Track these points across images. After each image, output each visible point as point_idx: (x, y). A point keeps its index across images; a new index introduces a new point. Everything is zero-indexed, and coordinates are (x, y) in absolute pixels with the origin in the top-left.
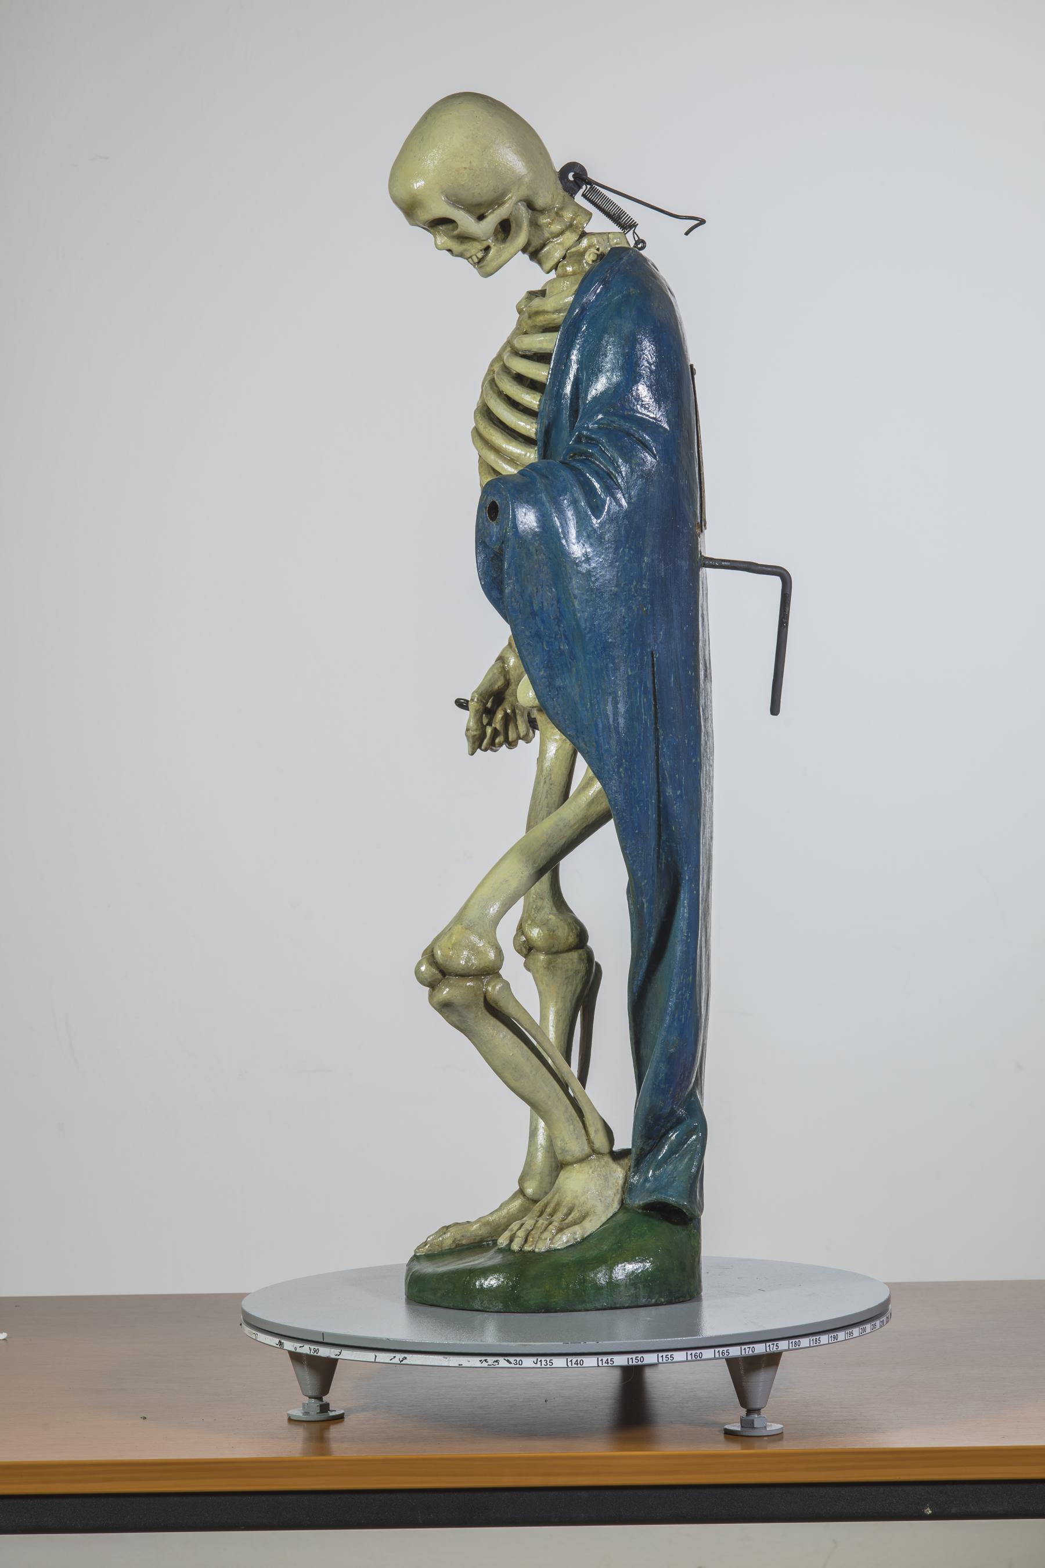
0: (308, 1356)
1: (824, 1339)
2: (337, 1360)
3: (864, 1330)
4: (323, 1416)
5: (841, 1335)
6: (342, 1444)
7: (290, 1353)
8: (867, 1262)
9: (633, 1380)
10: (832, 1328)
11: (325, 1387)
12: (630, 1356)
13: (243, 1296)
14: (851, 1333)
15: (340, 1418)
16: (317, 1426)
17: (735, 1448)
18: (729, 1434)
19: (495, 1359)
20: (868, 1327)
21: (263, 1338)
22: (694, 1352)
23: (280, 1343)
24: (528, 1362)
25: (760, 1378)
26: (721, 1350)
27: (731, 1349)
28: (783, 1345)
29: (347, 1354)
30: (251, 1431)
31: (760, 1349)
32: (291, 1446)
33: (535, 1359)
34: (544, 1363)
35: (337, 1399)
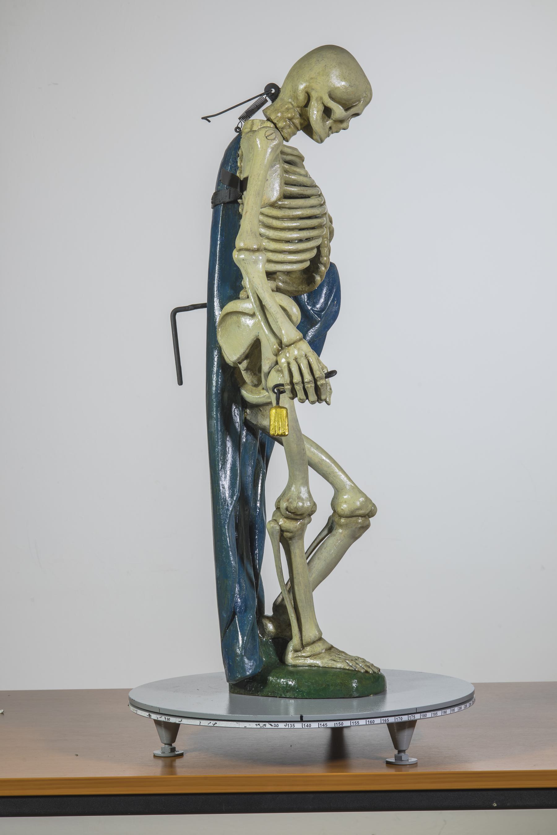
0: (164, 722)
1: (439, 713)
2: (179, 724)
3: (461, 708)
4: (172, 754)
5: (448, 711)
6: (183, 769)
7: (155, 720)
8: (461, 672)
9: (337, 735)
10: (443, 707)
11: (173, 738)
12: (336, 722)
13: (129, 690)
14: (454, 710)
15: (181, 755)
16: (169, 760)
17: (392, 771)
18: (388, 763)
19: (264, 723)
20: (463, 707)
21: (140, 712)
22: (370, 720)
23: (150, 715)
24: (281, 725)
25: (405, 734)
26: (384, 719)
27: (390, 718)
28: (417, 716)
29: (185, 721)
30: (133, 762)
31: (405, 718)
32: (155, 770)
33: (285, 724)
34: (290, 726)
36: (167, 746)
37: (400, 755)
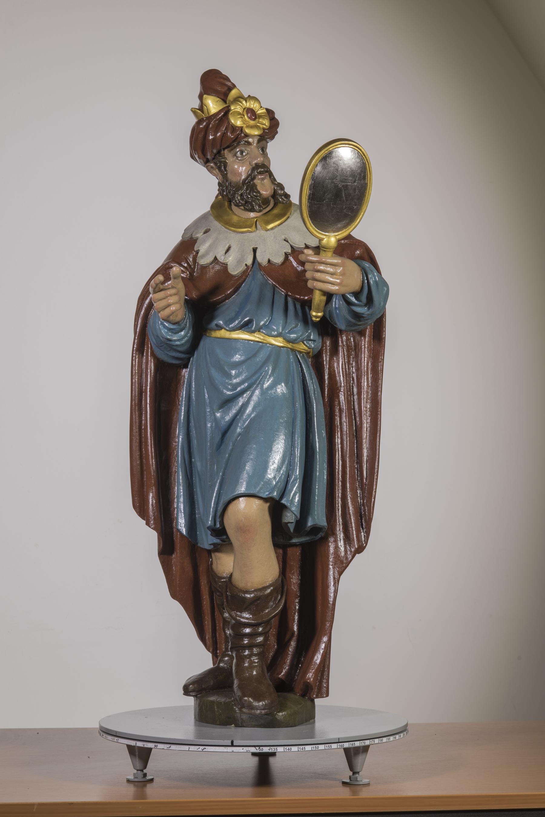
1: (392, 738)
5: (397, 737)
18: (344, 783)
36: (139, 772)
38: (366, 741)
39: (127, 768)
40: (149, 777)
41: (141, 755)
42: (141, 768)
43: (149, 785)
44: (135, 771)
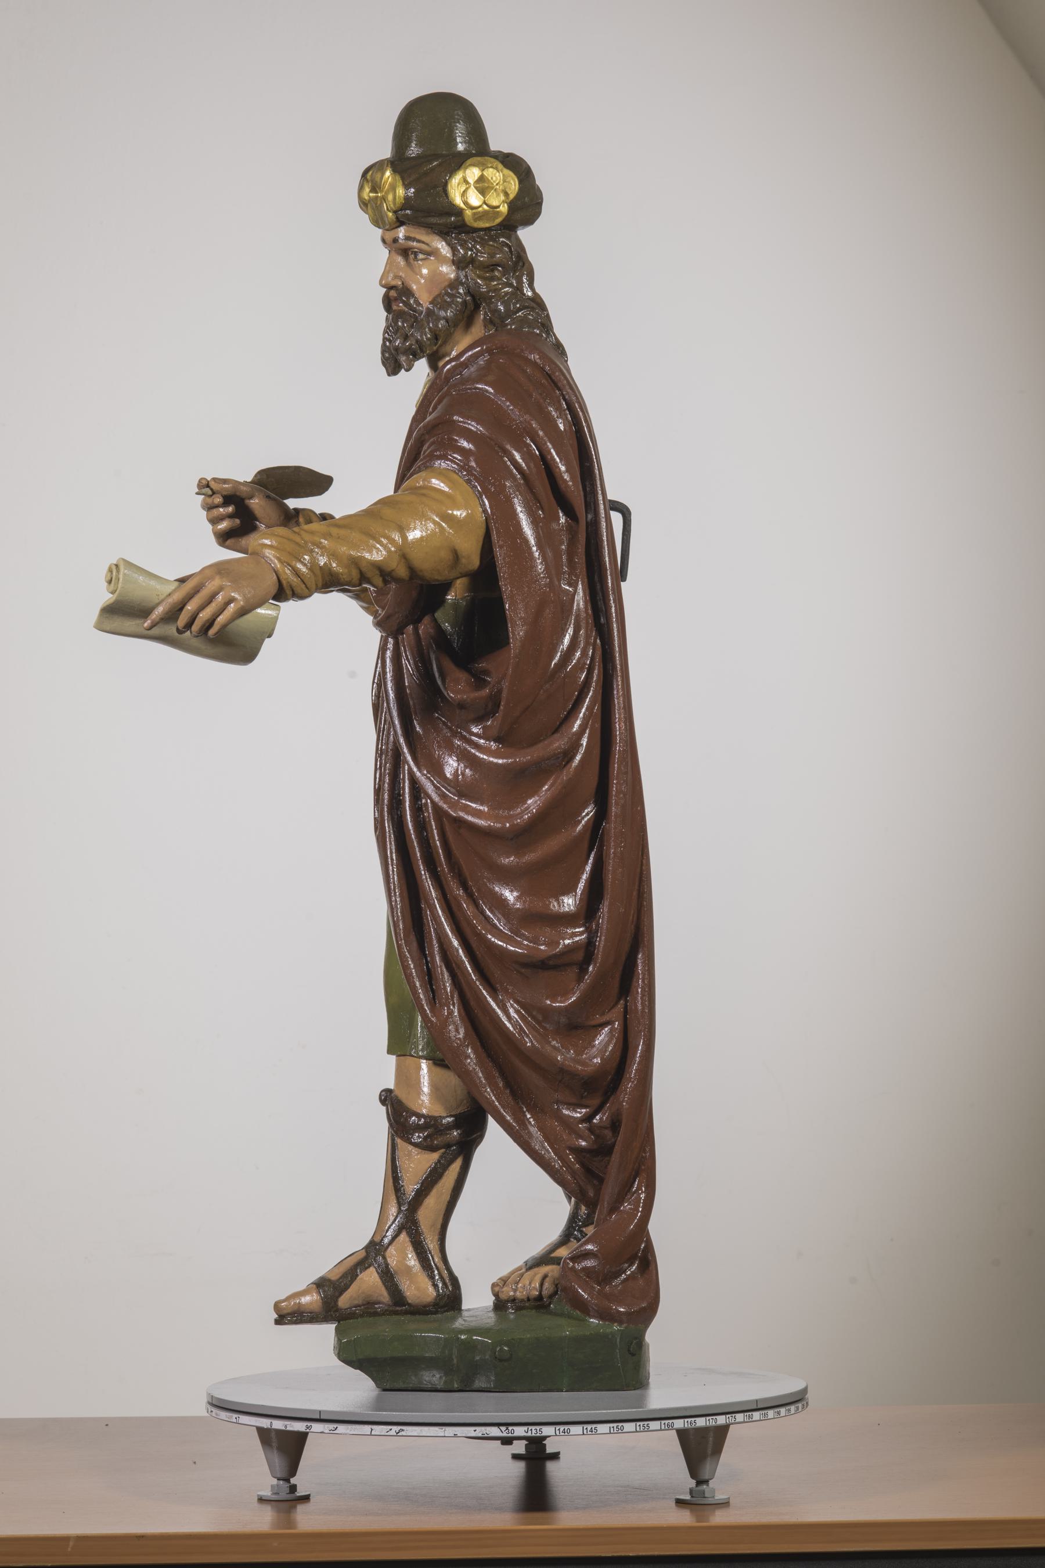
1: (771, 1413)
3: (798, 1408)
5: (783, 1411)
14: (789, 1410)
15: (306, 1498)
18: (680, 1502)
35: (302, 1481)
36: (281, 1482)
37: (700, 1488)
38: (718, 1417)
39: (260, 1474)
40: (301, 1492)
41: (287, 1448)
42: (284, 1475)
43: (301, 1508)
44: (275, 1481)
